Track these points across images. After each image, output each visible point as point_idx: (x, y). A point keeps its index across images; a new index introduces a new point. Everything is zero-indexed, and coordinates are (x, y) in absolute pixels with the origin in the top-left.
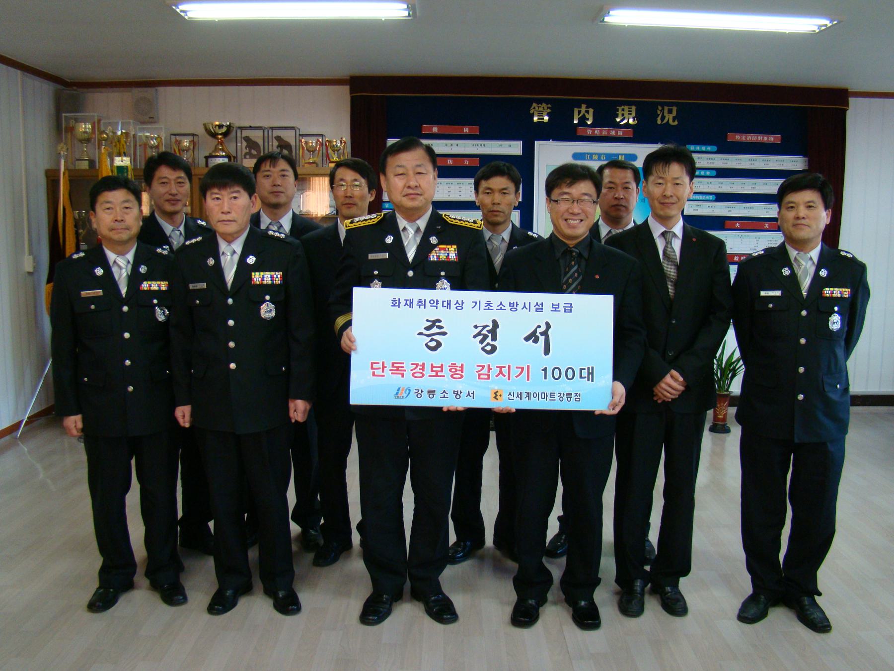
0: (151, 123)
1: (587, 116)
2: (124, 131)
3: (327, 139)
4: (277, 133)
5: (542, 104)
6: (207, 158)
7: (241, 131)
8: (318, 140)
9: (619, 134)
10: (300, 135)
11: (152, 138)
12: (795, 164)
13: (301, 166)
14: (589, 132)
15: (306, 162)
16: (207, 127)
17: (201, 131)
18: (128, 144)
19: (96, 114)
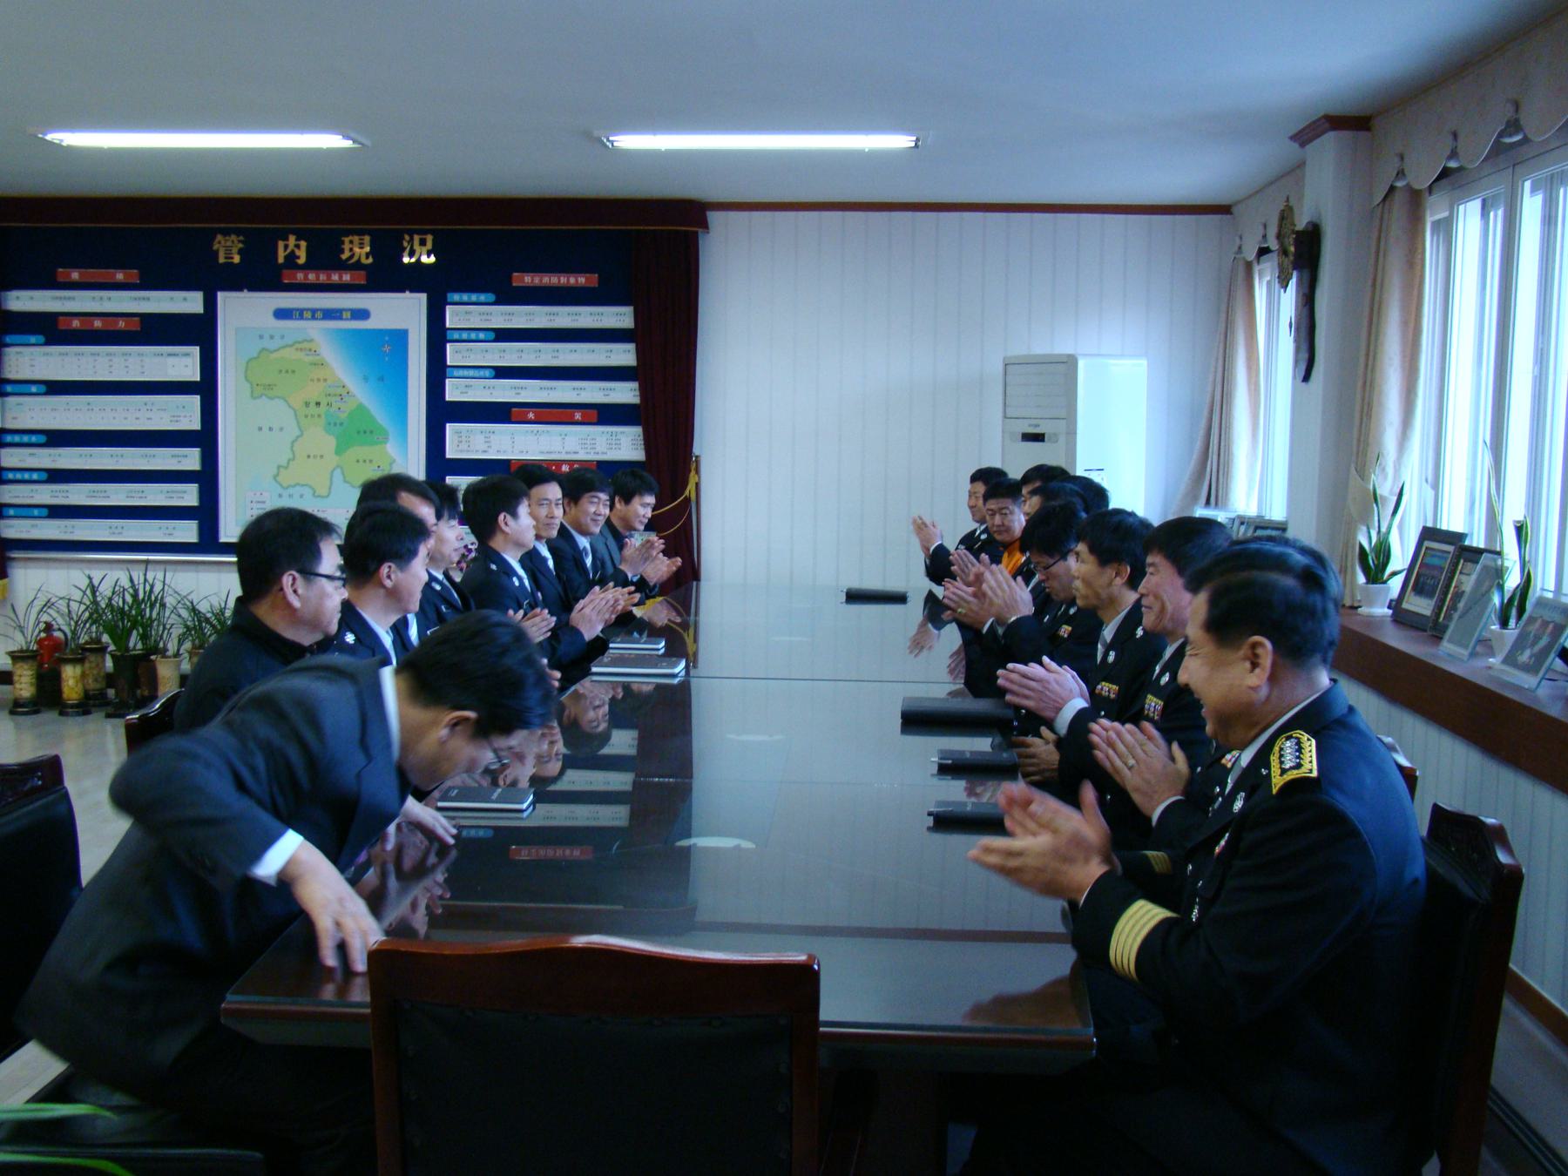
1: (297, 253)
5: (230, 236)
9: (344, 278)
12: (622, 318)
14: (300, 276)
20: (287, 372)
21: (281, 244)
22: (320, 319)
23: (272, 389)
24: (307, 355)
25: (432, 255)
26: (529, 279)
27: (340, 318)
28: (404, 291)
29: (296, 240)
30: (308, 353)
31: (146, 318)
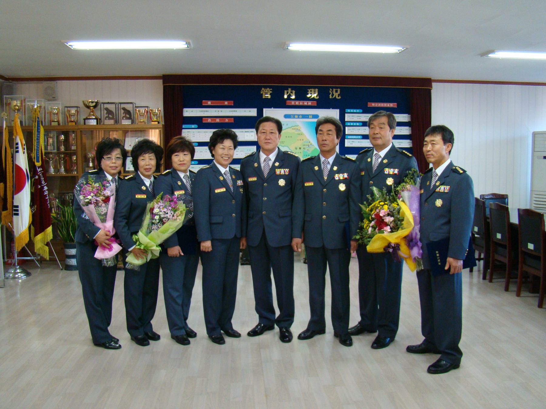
0: (54, 100)
2: (38, 105)
3: (150, 109)
4: (123, 106)
5: (267, 89)
6: (85, 119)
7: (104, 105)
8: (145, 110)
9: (309, 104)
10: (135, 107)
11: (54, 109)
12: (405, 118)
13: (136, 124)
14: (293, 103)
15: (139, 121)
16: (85, 103)
17: (81, 105)
18: (41, 112)
19: (23, 96)
20: (289, 137)
21: (286, 92)
22: (301, 118)
23: (283, 143)
24: (296, 131)
25: (340, 97)
26: (374, 105)
27: (308, 118)
28: (330, 109)
29: (291, 90)
30: (296, 130)
31: (235, 118)
